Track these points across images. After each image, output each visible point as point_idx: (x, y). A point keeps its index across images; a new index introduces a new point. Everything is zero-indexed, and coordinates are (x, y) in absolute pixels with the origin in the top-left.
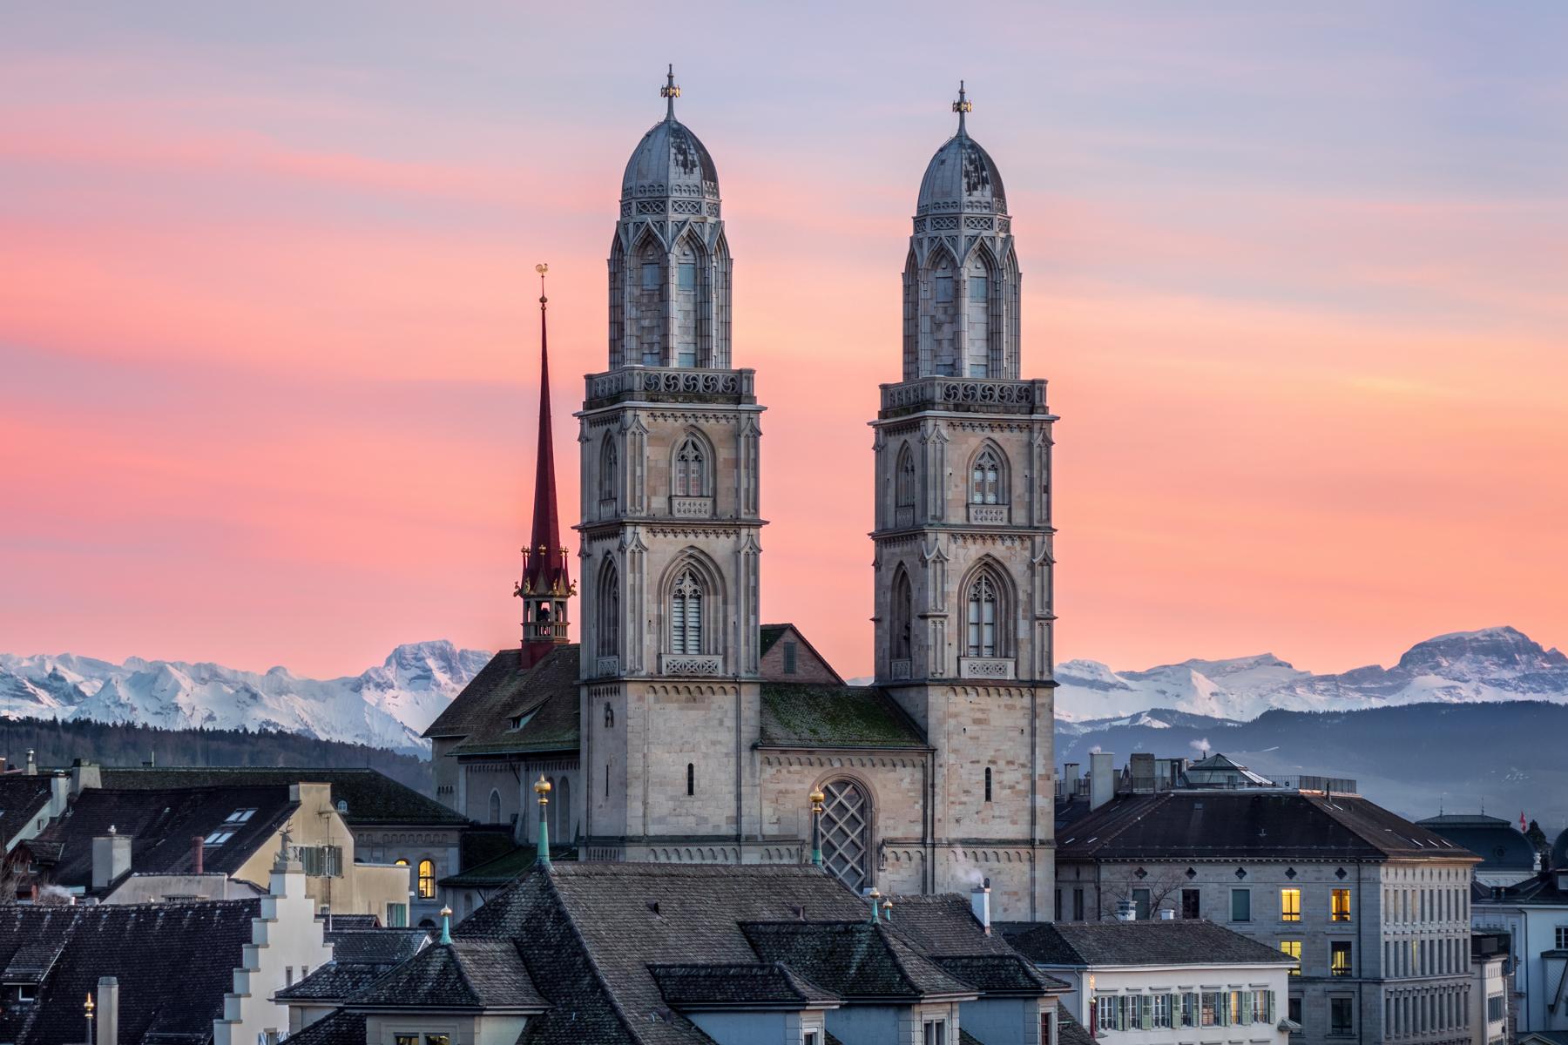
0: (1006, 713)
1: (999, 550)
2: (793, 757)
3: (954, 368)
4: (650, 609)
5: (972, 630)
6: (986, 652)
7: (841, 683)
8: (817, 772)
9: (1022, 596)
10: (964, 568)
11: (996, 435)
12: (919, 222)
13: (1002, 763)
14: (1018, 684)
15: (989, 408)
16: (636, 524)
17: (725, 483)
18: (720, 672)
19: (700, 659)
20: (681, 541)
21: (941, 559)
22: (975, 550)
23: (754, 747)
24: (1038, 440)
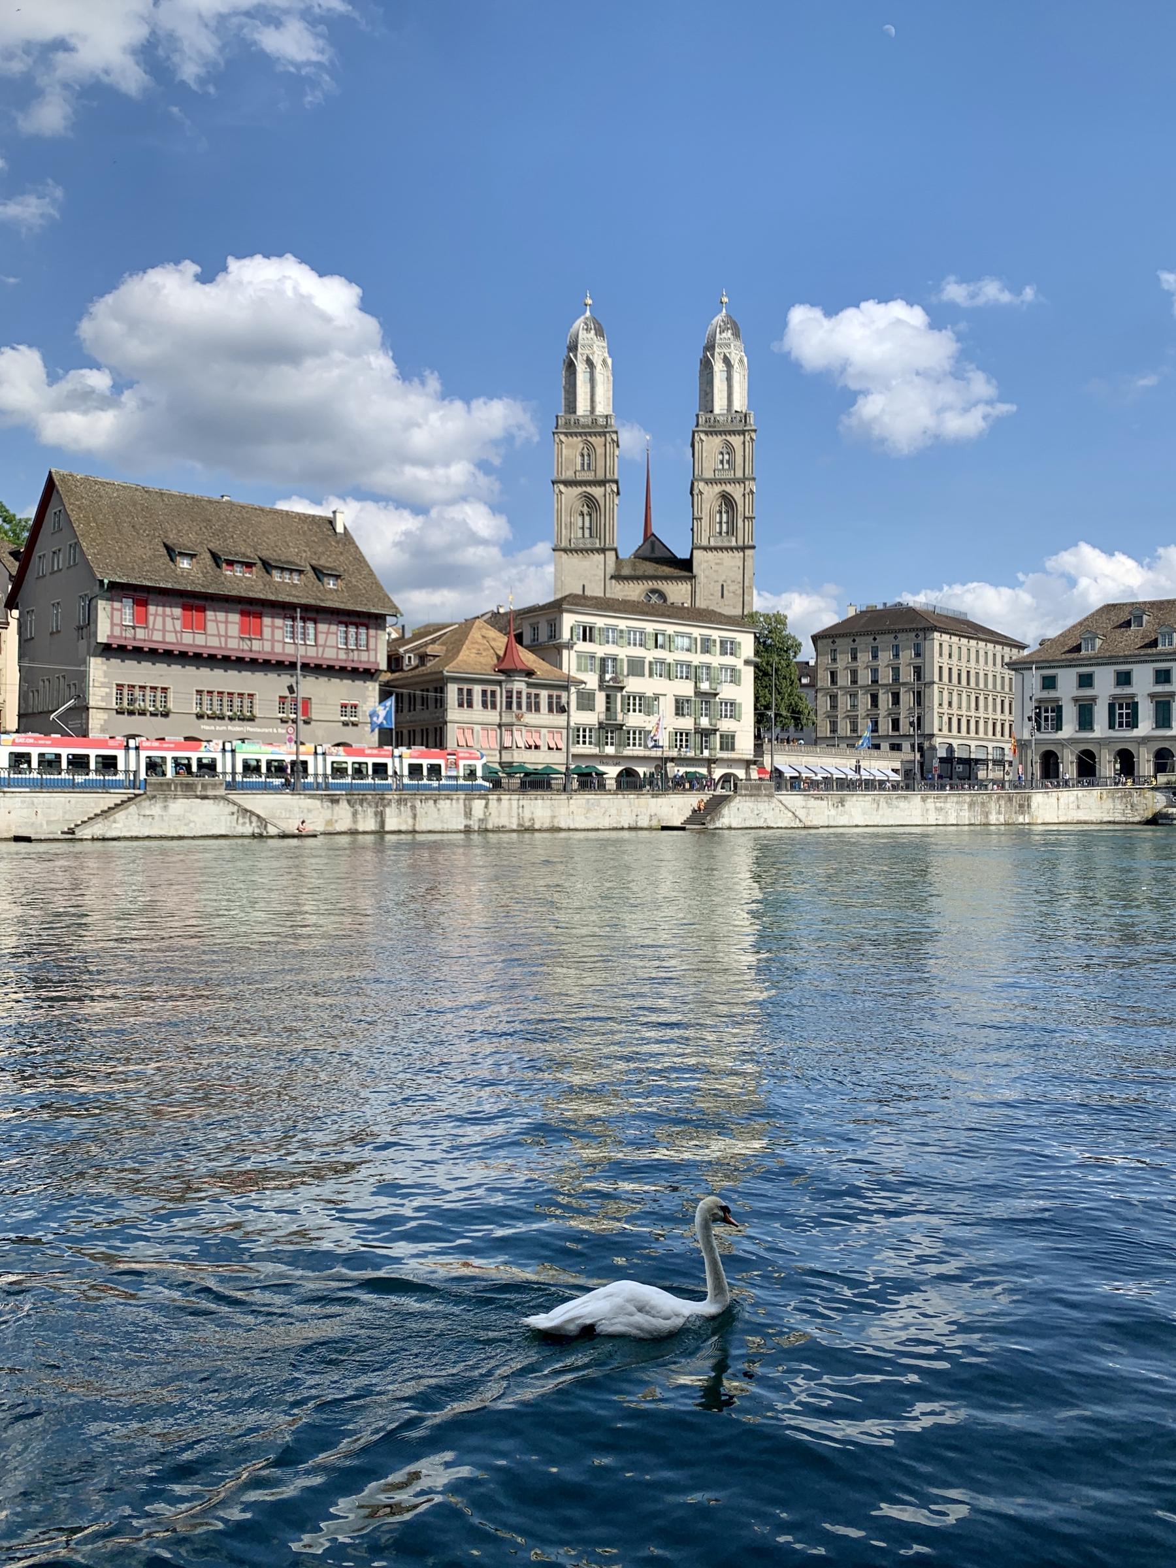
0: (732, 560)
1: (729, 488)
9: (740, 509)
10: (712, 496)
11: (730, 438)
13: (729, 582)
17: (600, 463)
20: (580, 490)
21: (701, 493)
22: (718, 489)
23: (612, 577)
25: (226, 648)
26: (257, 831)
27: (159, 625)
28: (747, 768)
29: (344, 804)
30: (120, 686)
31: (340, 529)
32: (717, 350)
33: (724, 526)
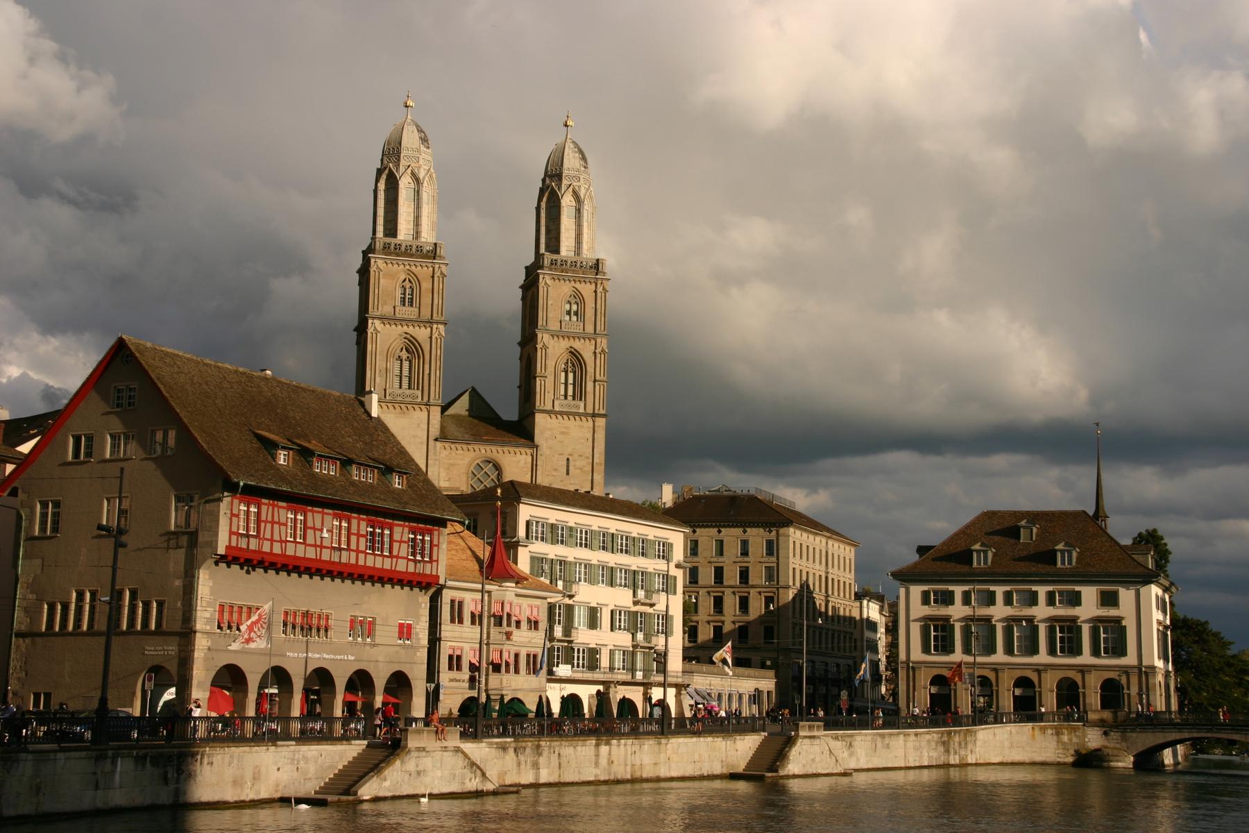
1: (577, 345)
2: (459, 446)
3: (556, 250)
4: (380, 364)
5: (563, 387)
6: (570, 398)
7: (499, 418)
8: (472, 454)
9: (590, 369)
12: (544, 181)
13: (576, 456)
14: (586, 415)
15: (574, 272)
16: (374, 318)
17: (426, 300)
18: (419, 400)
19: (409, 392)
20: (400, 329)
21: (545, 347)
22: (564, 344)
23: (436, 440)
24: (600, 289)
25: (320, 561)
26: (480, 788)
27: (268, 536)
28: (678, 695)
29: (511, 751)
30: (222, 606)
31: (374, 414)
32: (565, 182)
33: (570, 388)
